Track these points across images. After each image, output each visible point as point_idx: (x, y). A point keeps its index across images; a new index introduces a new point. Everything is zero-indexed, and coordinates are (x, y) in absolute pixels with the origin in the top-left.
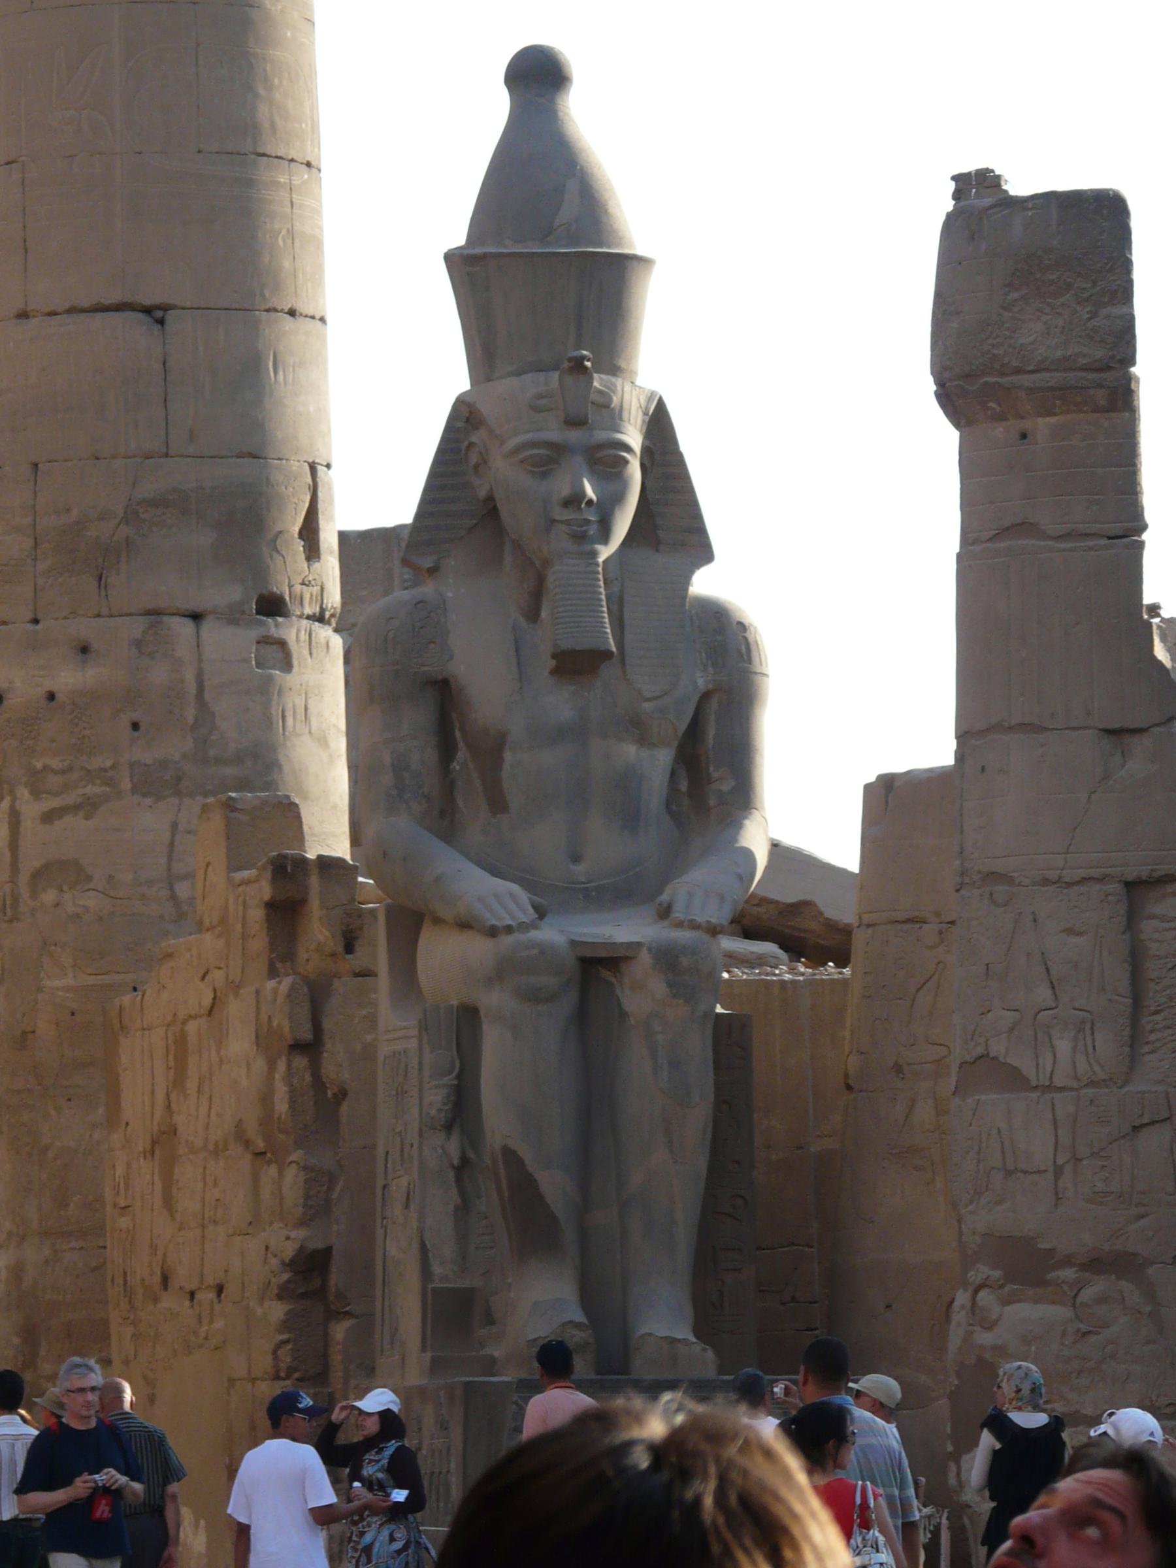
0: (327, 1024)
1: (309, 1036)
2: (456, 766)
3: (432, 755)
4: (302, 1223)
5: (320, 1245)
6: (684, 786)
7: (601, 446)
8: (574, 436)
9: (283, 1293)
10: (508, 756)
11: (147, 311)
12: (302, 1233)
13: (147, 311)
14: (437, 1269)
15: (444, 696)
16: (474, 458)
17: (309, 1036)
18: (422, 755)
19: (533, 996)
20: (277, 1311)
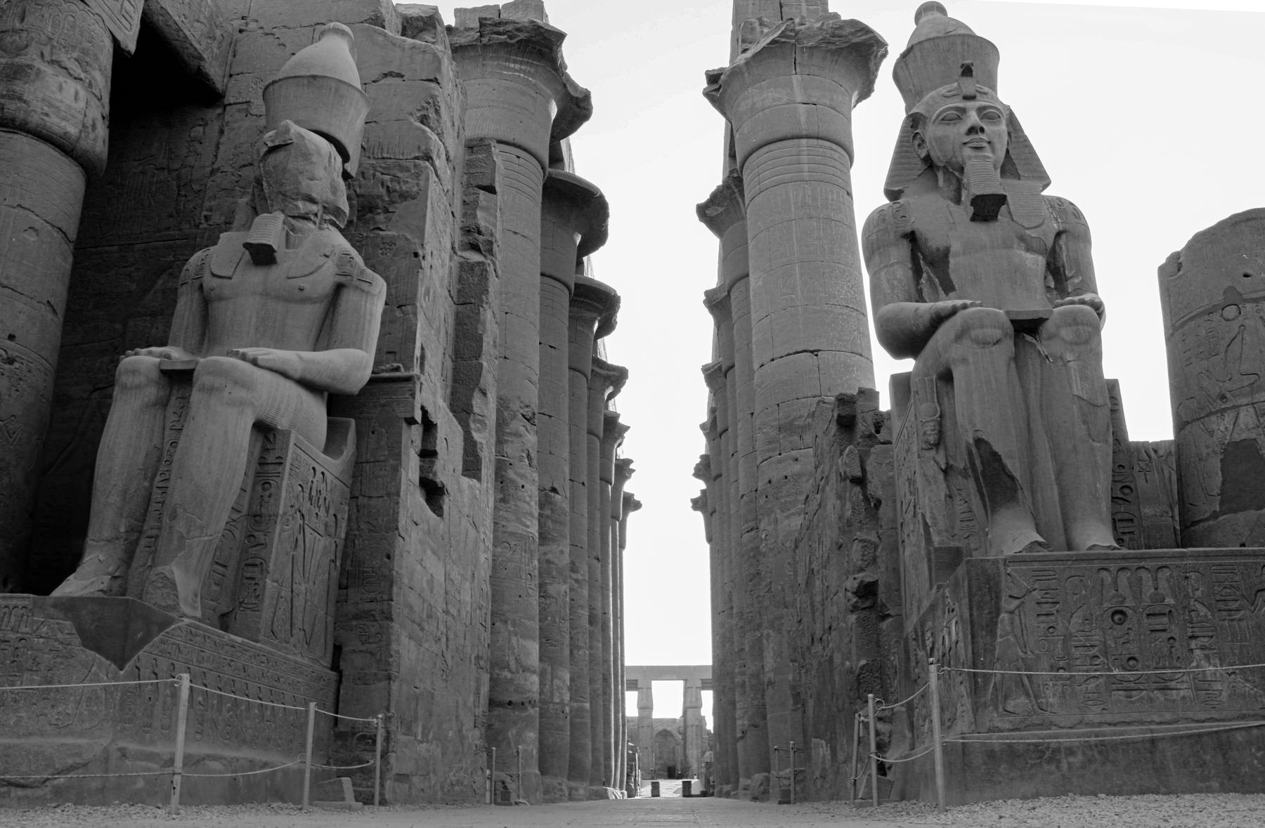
0: (868, 468)
1: (860, 474)
2: (923, 281)
3: (910, 273)
4: (861, 570)
5: (872, 580)
6: (1052, 285)
7: (985, 108)
8: (969, 104)
9: (854, 609)
10: (952, 261)
11: (812, 352)
12: (861, 575)
13: (812, 352)
14: (936, 539)
15: (912, 237)
16: (917, 142)
17: (860, 474)
18: (903, 272)
19: (984, 343)
20: (853, 618)
